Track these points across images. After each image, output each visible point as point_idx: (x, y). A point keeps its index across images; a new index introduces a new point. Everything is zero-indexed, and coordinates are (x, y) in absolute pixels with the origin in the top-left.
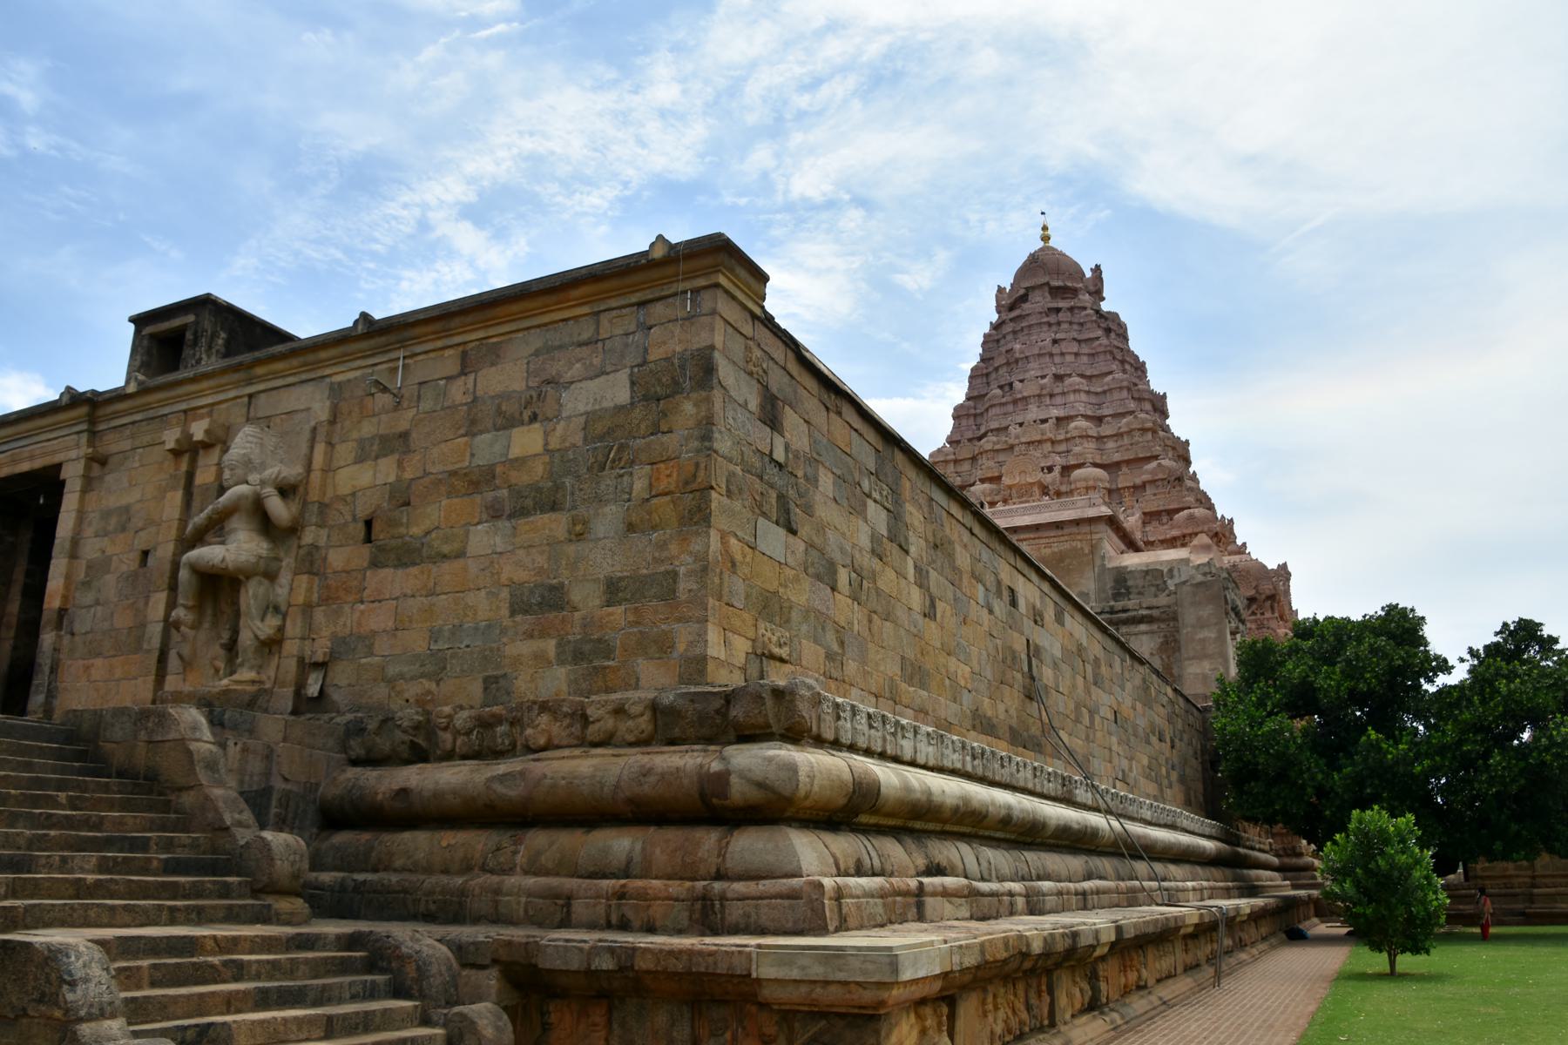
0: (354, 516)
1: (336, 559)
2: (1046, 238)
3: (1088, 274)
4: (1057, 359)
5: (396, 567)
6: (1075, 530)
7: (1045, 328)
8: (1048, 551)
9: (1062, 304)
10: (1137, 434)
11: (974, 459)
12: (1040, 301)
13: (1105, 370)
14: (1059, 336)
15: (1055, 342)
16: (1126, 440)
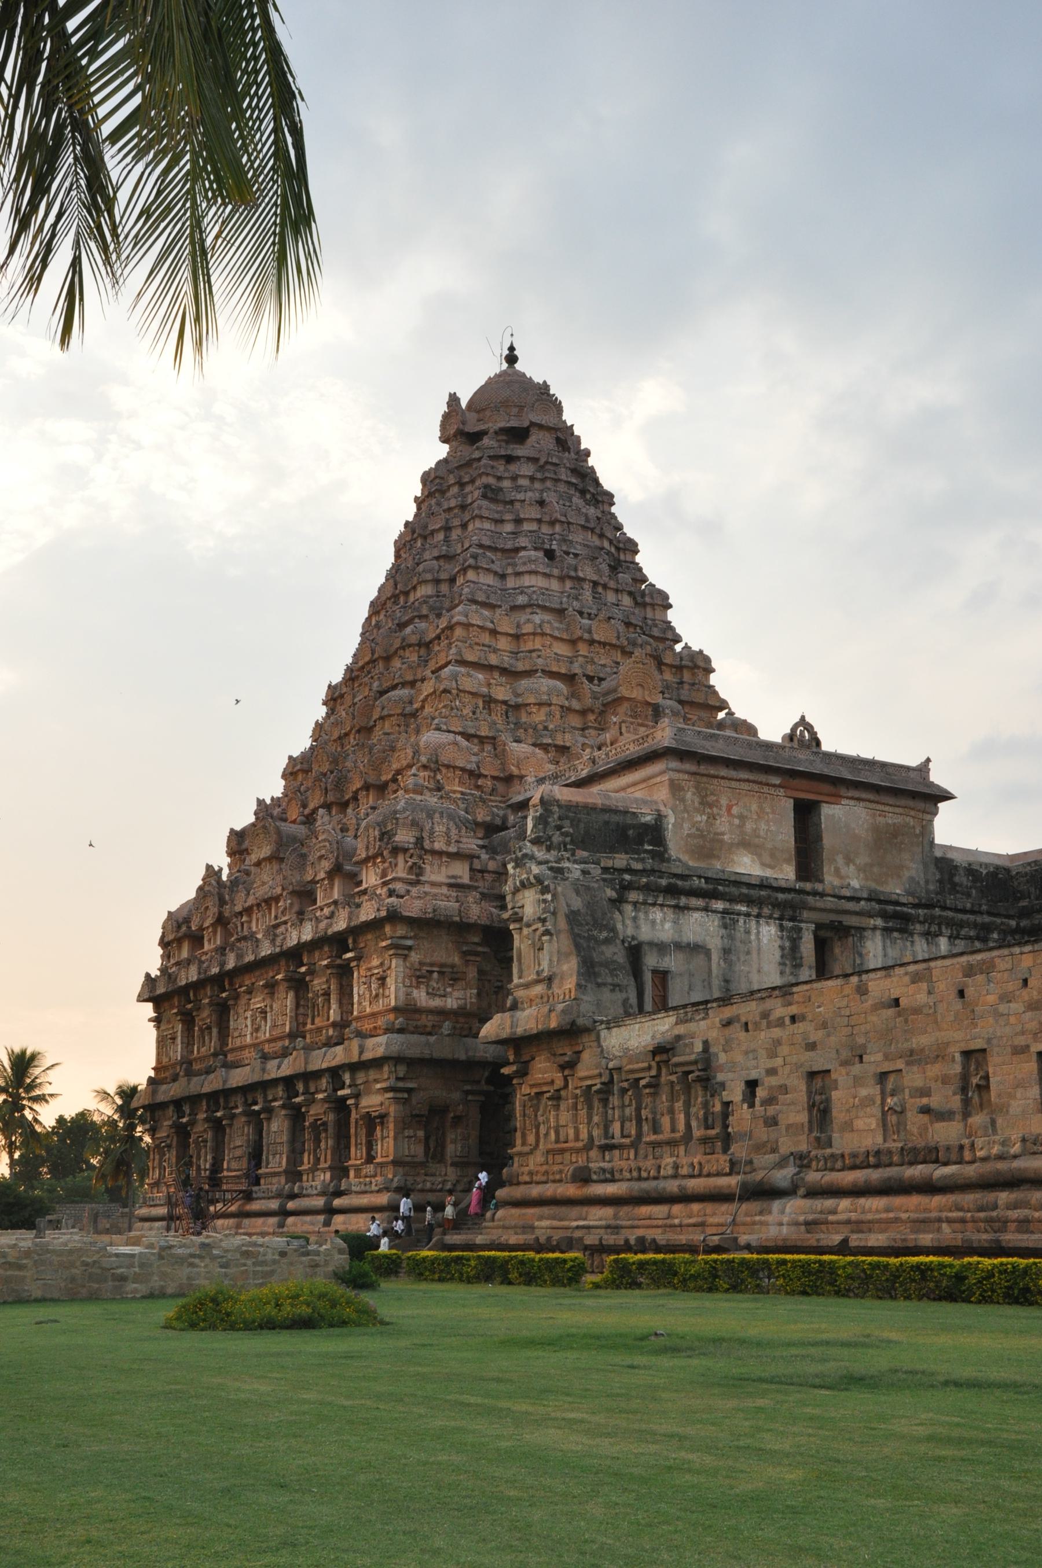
2: (512, 359)
6: (910, 803)
8: (881, 819)
16: (687, 676)
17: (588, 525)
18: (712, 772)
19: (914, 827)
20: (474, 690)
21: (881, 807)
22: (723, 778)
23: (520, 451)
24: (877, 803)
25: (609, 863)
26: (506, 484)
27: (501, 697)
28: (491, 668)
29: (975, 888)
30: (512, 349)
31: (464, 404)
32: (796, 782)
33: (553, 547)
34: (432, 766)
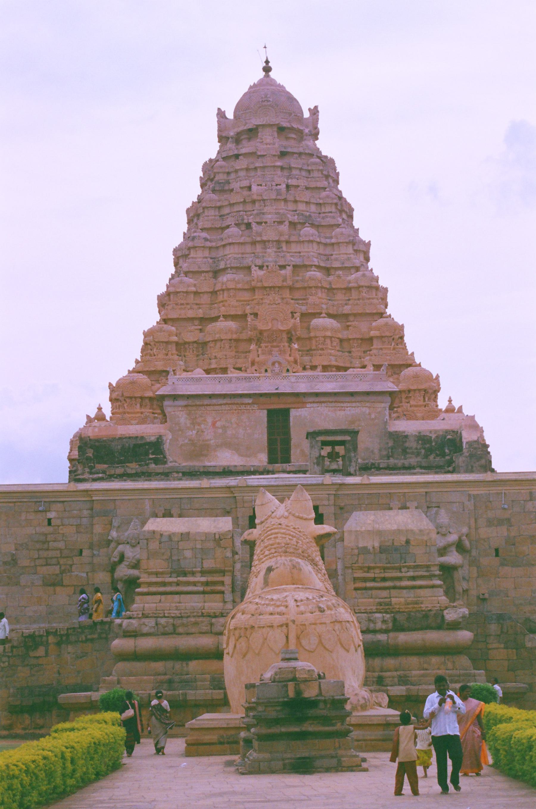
0: (490, 547)
1: (485, 561)
2: (267, 69)
3: (306, 114)
4: (291, 206)
5: (512, 567)
7: (279, 172)
8: (342, 413)
9: (292, 146)
10: (365, 290)
11: (214, 293)
12: (268, 143)
13: (332, 222)
14: (292, 182)
15: (288, 186)
16: (354, 294)
17: (279, 197)
18: (198, 403)
19: (370, 414)
20: (166, 340)
21: (342, 405)
22: (207, 405)
23: (246, 148)
24: (336, 402)
25: (113, 472)
26: (233, 176)
27: (192, 339)
28: (192, 319)
29: (424, 448)
30: (267, 62)
31: (230, 115)
32: (262, 399)
33: (250, 221)
34: (121, 398)
